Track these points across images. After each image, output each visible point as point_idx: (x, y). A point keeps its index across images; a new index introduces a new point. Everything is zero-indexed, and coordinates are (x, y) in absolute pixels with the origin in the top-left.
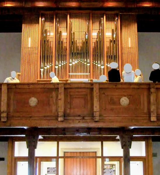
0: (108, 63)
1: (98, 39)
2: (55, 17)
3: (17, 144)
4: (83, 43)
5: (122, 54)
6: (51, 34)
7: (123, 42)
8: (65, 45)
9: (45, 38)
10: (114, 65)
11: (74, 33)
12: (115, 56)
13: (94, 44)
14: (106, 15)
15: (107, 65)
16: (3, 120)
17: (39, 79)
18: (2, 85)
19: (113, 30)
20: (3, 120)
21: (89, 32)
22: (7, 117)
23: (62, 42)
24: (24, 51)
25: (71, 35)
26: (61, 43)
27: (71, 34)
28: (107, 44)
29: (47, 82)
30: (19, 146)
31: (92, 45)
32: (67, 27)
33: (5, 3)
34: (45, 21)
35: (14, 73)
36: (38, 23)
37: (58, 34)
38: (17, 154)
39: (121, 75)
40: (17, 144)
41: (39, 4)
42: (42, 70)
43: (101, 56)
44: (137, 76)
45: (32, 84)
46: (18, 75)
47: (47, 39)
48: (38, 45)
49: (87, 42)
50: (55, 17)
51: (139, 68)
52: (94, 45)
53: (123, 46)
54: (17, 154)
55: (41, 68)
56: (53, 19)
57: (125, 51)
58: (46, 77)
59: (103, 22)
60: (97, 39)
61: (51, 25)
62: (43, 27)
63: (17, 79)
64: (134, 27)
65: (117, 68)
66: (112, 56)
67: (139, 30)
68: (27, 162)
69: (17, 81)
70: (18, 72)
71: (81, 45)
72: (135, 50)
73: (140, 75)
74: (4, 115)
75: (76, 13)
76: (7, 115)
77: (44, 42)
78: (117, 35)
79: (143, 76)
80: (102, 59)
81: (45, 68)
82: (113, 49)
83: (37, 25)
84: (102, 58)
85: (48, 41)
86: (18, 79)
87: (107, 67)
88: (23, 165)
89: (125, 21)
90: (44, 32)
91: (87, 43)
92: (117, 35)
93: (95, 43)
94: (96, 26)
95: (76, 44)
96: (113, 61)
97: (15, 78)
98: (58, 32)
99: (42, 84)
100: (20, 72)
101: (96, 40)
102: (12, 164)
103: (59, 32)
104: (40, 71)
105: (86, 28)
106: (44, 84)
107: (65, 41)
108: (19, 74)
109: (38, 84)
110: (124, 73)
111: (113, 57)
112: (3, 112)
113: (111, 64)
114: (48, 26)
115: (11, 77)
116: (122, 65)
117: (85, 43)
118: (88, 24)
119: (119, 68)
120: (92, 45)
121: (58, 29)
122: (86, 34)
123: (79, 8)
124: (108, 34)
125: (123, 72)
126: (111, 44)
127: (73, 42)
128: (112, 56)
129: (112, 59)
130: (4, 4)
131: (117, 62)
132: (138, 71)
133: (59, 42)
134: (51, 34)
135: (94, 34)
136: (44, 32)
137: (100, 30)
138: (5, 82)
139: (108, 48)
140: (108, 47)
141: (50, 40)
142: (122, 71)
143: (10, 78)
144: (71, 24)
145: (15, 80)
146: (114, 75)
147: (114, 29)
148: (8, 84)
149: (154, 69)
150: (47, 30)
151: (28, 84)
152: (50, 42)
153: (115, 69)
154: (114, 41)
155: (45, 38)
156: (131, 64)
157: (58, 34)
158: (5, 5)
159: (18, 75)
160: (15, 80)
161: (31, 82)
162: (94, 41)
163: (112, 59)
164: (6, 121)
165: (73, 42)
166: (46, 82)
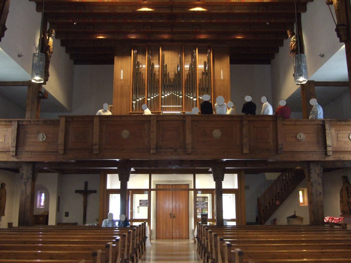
0: (201, 96)
1: (190, 72)
2: (147, 49)
3: (109, 176)
4: (176, 75)
5: (214, 86)
6: (144, 66)
7: (216, 75)
8: (157, 77)
9: (137, 70)
10: (206, 98)
11: (166, 65)
12: (207, 88)
13: (186, 76)
14: (198, 48)
15: (199, 97)
16: (95, 152)
17: (131, 112)
18: (95, 117)
19: (205, 62)
20: (95, 152)
21: (181, 64)
22: (99, 150)
23: (154, 74)
24: (117, 84)
25: (164, 67)
26: (153, 75)
27: (164, 66)
28: (199, 76)
29: (140, 115)
30: (112, 180)
31: (185, 77)
32: (159, 59)
33: (98, 35)
34: (137, 53)
35: (106, 105)
36: (131, 55)
37: (151, 66)
38: (109, 187)
39: (214, 107)
40: (109, 176)
41: (131, 37)
42: (134, 102)
43: (194, 88)
44: (229, 109)
45: (125, 116)
46: (110, 107)
47: (140, 71)
48: (130, 77)
49: (179, 74)
50: (147, 49)
51: (231, 101)
52: (186, 77)
53: (216, 78)
54: (109, 187)
55: (133, 100)
56: (146, 51)
57: (218, 84)
58: (138, 110)
59: (195, 55)
60: (189, 71)
61: (144, 57)
62: (135, 59)
63: (109, 111)
64: (227, 61)
65: (209, 101)
66: (204, 88)
67: (231, 62)
68: (119, 195)
69: (109, 113)
70: (111, 105)
71: (173, 77)
72: (227, 83)
73: (233, 108)
74: (97, 147)
75: (169, 46)
76: (100, 147)
77: (136, 73)
78: (209, 67)
79: (235, 109)
80: (195, 91)
81: (138, 100)
82: (205, 81)
83: (129, 57)
84: (195, 90)
85: (140, 73)
86: (110, 111)
87: (199, 98)
88: (115, 197)
89: (218, 56)
90: (136, 64)
91: (179, 74)
92: (209, 67)
93: (187, 75)
94: (189, 59)
95: (169, 77)
96: (206, 94)
97: (108, 110)
98: (150, 64)
99: (134, 116)
100: (112, 105)
101: (189, 72)
102: (104, 196)
103: (151, 64)
104: (132, 103)
105: (179, 60)
106: (137, 116)
107: (157, 73)
108: (111, 106)
109: (131, 116)
110: (217, 105)
111: (205, 90)
112: (95, 144)
113: (203, 96)
114: (140, 58)
115: (103, 110)
116: (215, 98)
117: (178, 75)
118: (181, 56)
119: (211, 101)
120: (185, 77)
121: (150, 61)
122: (178, 67)
123: (171, 41)
124: (200, 67)
125: (216, 104)
126: (204, 76)
127: (165, 74)
128: (204, 88)
129: (204, 91)
130: (97, 37)
131: (209, 95)
132: (230, 103)
133: (151, 74)
134: (144, 66)
135: (187, 66)
136: (136, 64)
137: (192, 62)
138: (97, 114)
139: (200, 80)
140: (201, 79)
141: (143, 72)
142: (214, 104)
143: (102, 110)
144: (163, 56)
145: (108, 112)
146: (207, 107)
147: (207, 61)
148: (101, 117)
149: (247, 102)
150: (139, 62)
151: (120, 117)
152: (143, 74)
153: (207, 101)
154: (206, 73)
155: (137, 70)
156: (224, 96)
157: (151, 66)
158: (98, 38)
159: (110, 107)
160: (108, 112)
161: (124, 114)
162: (187, 73)
163: (204, 91)
164: (98, 153)
165: (165, 74)
166: (138, 115)
